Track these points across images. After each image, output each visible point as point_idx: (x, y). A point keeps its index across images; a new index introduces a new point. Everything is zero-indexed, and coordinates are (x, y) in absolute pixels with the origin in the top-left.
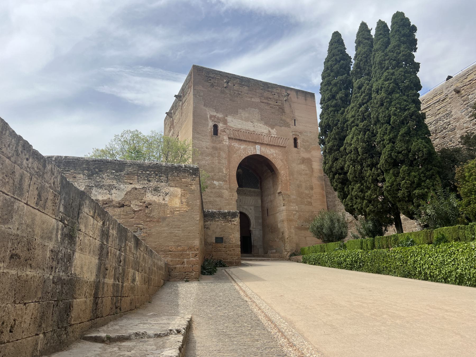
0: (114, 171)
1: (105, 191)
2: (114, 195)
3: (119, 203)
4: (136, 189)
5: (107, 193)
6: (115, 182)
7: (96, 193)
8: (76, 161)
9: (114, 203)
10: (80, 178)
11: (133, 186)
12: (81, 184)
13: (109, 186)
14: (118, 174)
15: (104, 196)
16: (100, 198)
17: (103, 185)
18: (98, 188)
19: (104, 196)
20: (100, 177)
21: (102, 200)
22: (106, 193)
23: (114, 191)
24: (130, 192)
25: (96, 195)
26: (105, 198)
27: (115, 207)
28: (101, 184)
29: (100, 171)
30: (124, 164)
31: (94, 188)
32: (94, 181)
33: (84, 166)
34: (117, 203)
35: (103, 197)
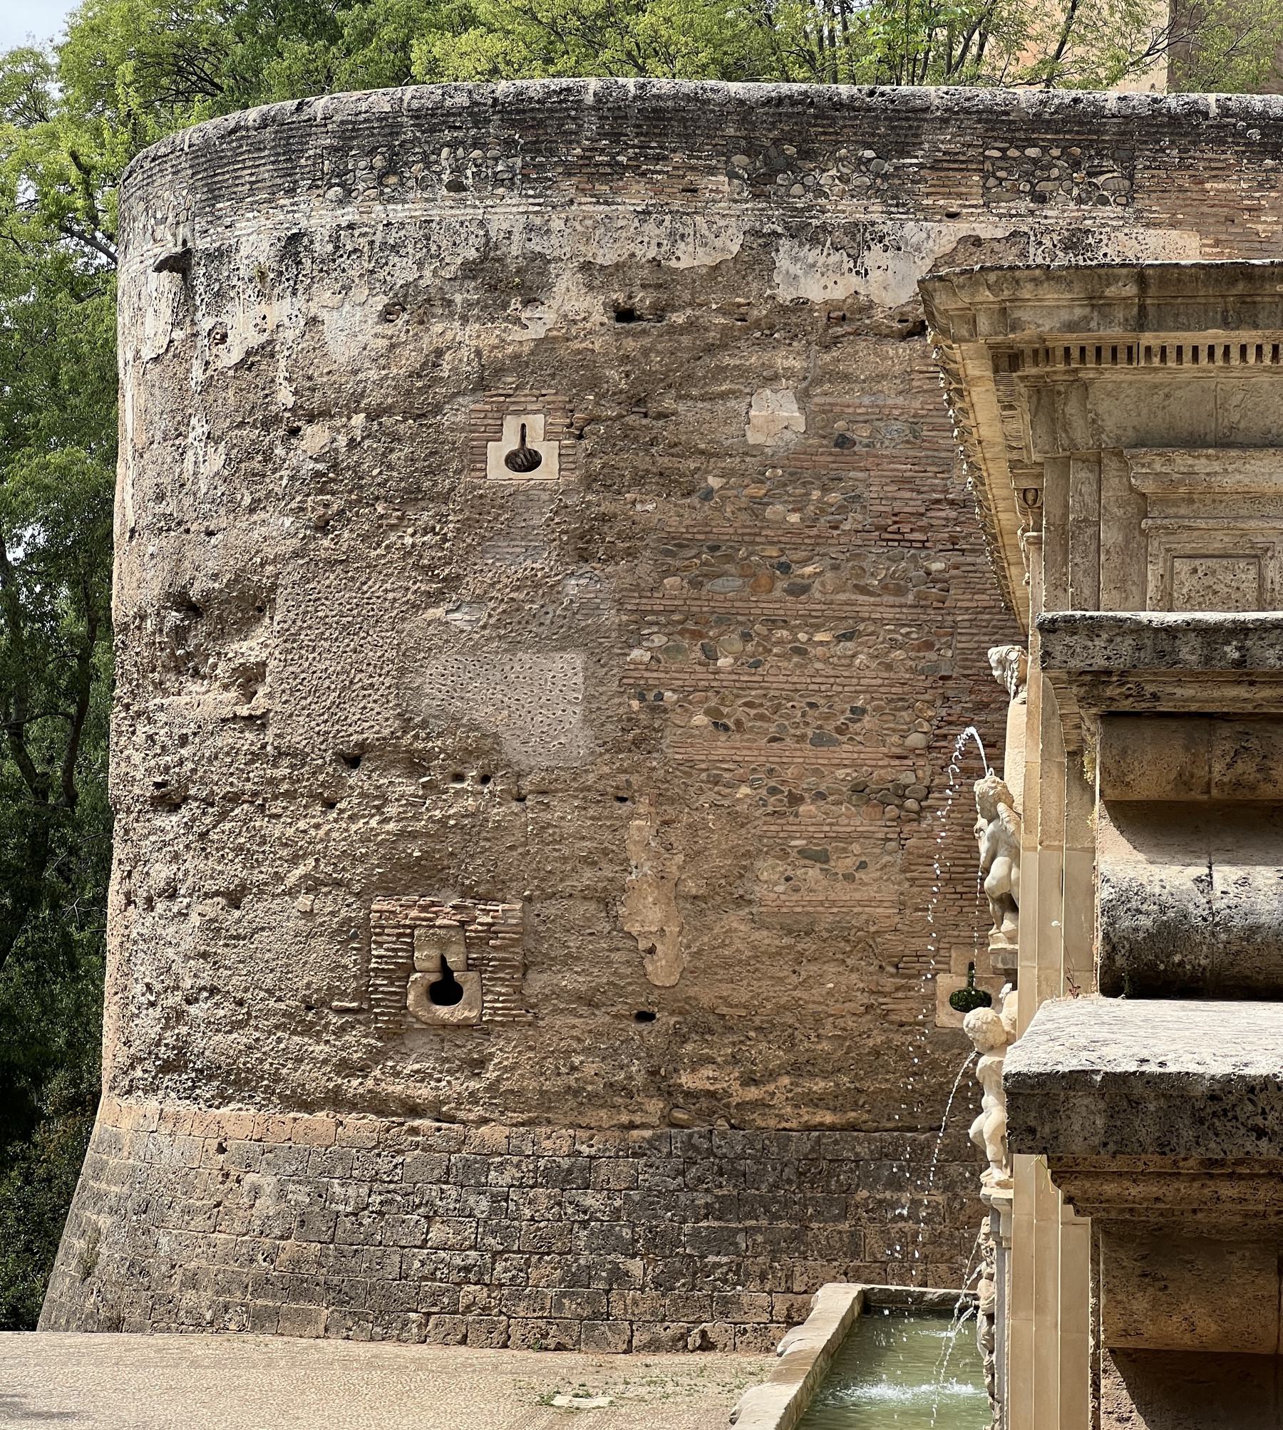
0: (869, 154)
1: (835, 257)
2: (875, 275)
3: (902, 314)
4: (977, 242)
5: (846, 266)
6: (876, 212)
7: (796, 269)
8: (691, 106)
9: (879, 315)
10: (717, 191)
11: (962, 228)
12: (722, 223)
13: (853, 229)
14: (888, 167)
15: (830, 285)
16: (815, 290)
17: (823, 227)
18: (801, 245)
19: (830, 285)
20: (807, 189)
21: (826, 303)
22: (840, 267)
23: (875, 256)
24: (950, 258)
25: (796, 277)
26: (838, 293)
27: (882, 335)
28: (814, 222)
29: (806, 154)
30: (915, 110)
31: (785, 244)
32: (779, 207)
33: (731, 131)
34: (892, 318)
35: (825, 287)
